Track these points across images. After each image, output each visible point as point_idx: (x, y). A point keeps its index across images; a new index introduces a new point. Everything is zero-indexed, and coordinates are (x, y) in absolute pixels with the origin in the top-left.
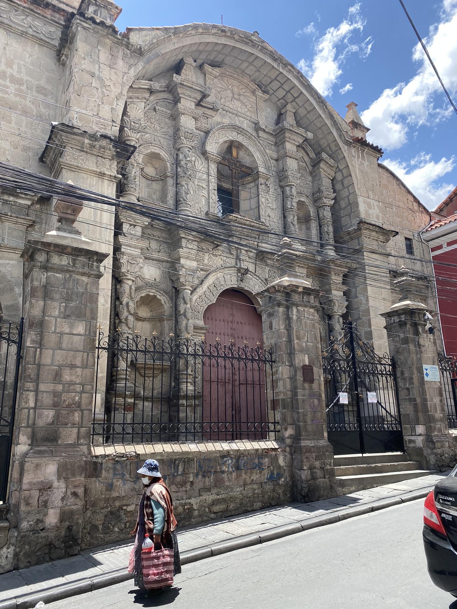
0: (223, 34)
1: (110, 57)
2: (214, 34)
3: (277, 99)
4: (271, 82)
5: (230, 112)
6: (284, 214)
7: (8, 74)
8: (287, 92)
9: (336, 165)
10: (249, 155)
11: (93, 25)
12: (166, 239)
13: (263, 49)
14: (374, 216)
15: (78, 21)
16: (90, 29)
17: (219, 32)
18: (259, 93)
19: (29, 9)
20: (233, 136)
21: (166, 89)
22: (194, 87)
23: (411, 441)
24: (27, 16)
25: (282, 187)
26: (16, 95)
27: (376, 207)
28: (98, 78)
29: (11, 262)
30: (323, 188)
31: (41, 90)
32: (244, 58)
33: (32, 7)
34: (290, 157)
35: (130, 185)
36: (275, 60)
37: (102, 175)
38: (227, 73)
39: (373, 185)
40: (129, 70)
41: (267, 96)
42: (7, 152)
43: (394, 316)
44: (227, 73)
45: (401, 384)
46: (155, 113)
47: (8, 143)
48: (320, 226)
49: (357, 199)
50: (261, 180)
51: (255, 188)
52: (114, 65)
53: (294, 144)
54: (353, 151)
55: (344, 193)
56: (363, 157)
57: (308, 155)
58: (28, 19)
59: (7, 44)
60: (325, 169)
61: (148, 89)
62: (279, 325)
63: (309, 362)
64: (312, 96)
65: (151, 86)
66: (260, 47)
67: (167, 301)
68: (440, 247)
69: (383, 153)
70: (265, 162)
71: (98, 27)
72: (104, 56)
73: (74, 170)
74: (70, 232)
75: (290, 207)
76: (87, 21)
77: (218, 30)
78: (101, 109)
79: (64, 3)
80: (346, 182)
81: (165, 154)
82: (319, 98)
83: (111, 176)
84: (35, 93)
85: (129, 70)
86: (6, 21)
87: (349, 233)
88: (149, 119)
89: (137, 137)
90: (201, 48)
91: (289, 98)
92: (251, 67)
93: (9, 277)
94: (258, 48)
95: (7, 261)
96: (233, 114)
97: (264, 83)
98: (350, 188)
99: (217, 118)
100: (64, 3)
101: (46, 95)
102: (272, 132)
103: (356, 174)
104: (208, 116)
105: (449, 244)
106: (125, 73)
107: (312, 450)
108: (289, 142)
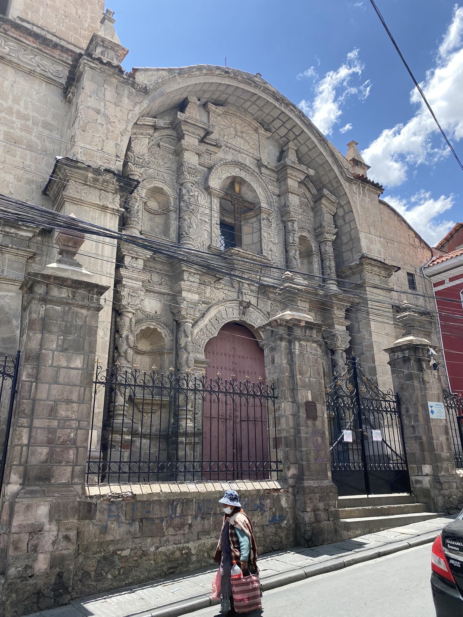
0: (227, 75)
1: (116, 96)
2: (217, 75)
3: (279, 137)
4: (274, 120)
5: (233, 149)
6: (286, 249)
7: (15, 110)
8: (289, 130)
9: (337, 201)
10: (251, 191)
11: (100, 65)
12: (168, 271)
13: (266, 90)
14: (376, 251)
15: (85, 61)
16: (97, 68)
17: (223, 73)
18: (262, 131)
19: (37, 49)
20: (235, 172)
21: (170, 126)
22: (197, 124)
23: (417, 482)
24: (36, 55)
25: (284, 222)
26: (22, 130)
27: (377, 243)
28: (103, 115)
29: (11, 294)
30: (325, 224)
31: (47, 126)
32: (246, 98)
33: (40, 47)
34: (292, 193)
35: (132, 219)
36: (277, 100)
37: (104, 208)
38: (231, 112)
39: (374, 221)
40: (134, 108)
41: (269, 134)
42: (10, 185)
43: (397, 352)
44: (231, 112)
45: (406, 422)
46: (158, 149)
47: (11, 176)
48: (322, 261)
49: (358, 234)
50: (263, 216)
51: (257, 223)
52: (119, 103)
53: (296, 180)
54: (354, 187)
55: (346, 228)
56: (364, 193)
57: (310, 191)
58: (37, 58)
59: (15, 82)
60: (327, 204)
61: (152, 125)
62: (282, 360)
63: (313, 398)
64: (314, 135)
65: (155, 123)
66: (262, 88)
67: (167, 335)
68: (442, 283)
69: (383, 190)
70: (267, 197)
71: (105, 67)
72: (109, 93)
73: (77, 203)
74: (71, 265)
75: (291, 242)
76: (95, 62)
77: (222, 71)
78: (105, 144)
79: (72, 44)
80: (347, 218)
81: (168, 188)
82: (320, 136)
83: (113, 209)
84: (40, 129)
85: (134, 108)
86: (15, 60)
87: (351, 268)
88: (153, 154)
89: (141, 172)
90: (205, 88)
91: (291, 136)
92: (254, 107)
93: (7, 310)
94: (260, 88)
95: (6, 293)
96: (236, 151)
97: (266, 121)
98: (352, 224)
99: (220, 154)
100: (72, 44)
101: (51, 131)
102: (274, 168)
103: (357, 210)
104: (211, 153)
105: (451, 280)
106: (130, 110)
107: (316, 490)
108: (291, 178)
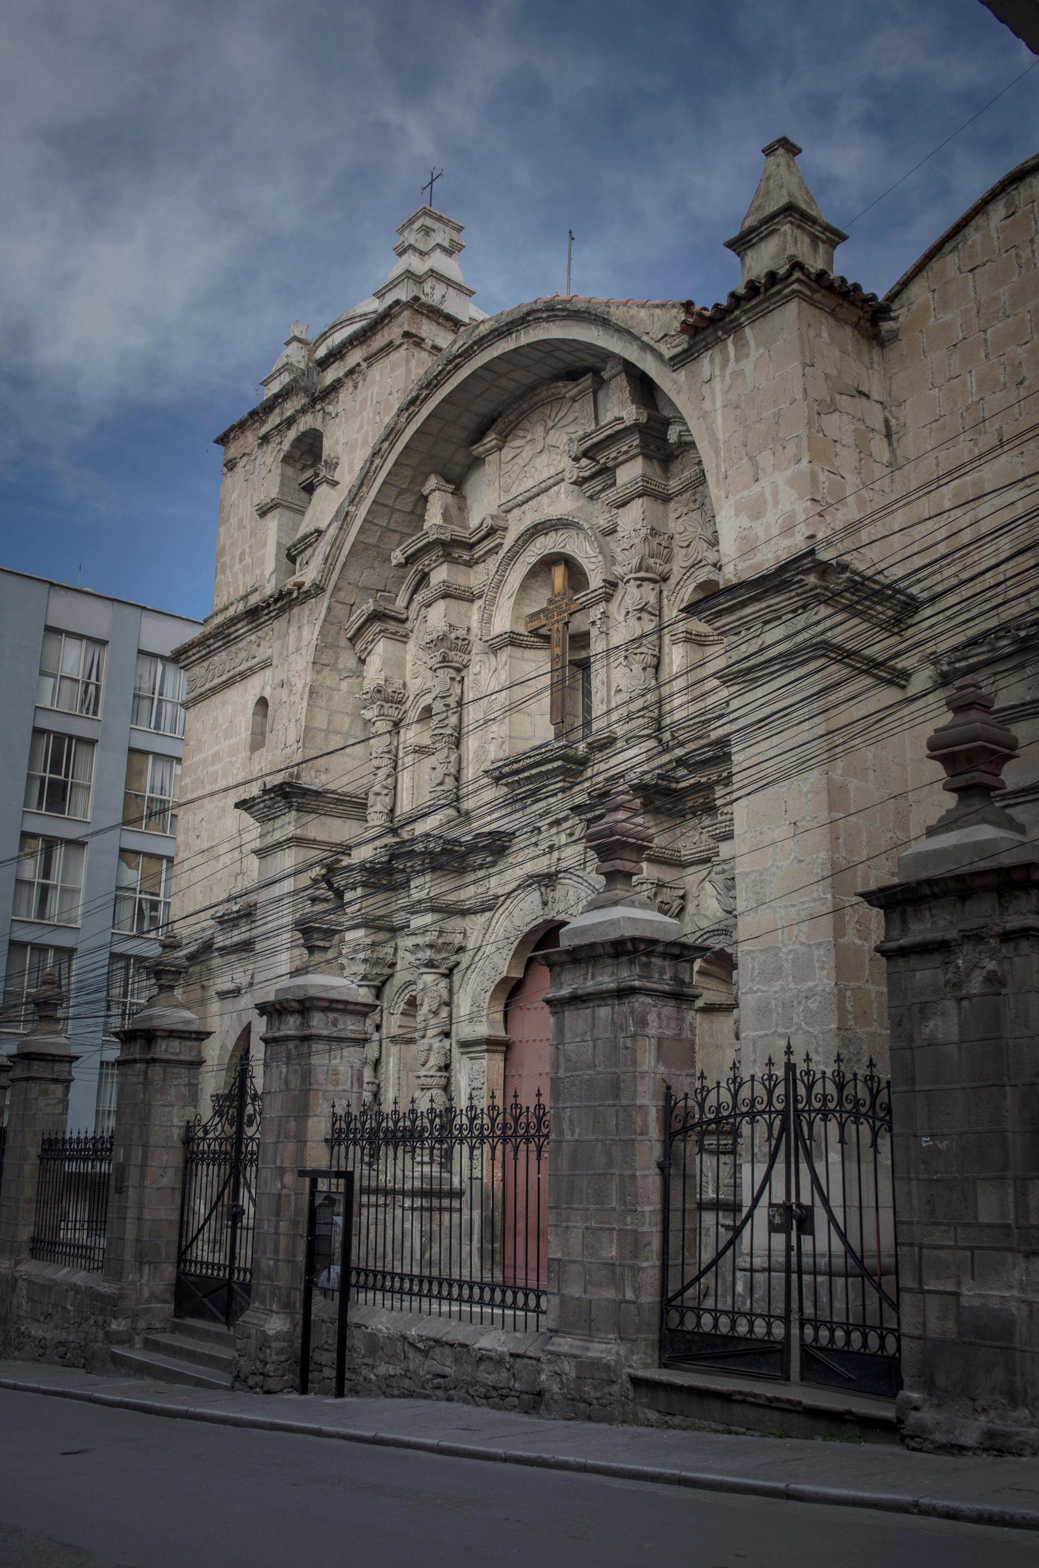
18: (571, 390)
41: (587, 381)
44: (512, 417)
89: (376, 713)
96: (538, 495)
103: (713, 435)
